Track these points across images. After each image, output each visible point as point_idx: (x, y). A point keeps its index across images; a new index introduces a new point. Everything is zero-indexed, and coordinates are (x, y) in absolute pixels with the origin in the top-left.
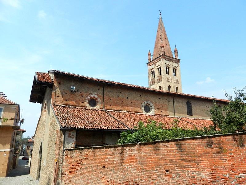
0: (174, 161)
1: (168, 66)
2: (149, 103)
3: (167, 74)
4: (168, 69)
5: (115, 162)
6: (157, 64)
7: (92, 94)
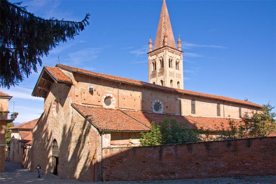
0: (203, 157)
2: (158, 101)
3: (170, 67)
4: (170, 61)
5: (154, 159)
6: (160, 55)
7: (107, 93)
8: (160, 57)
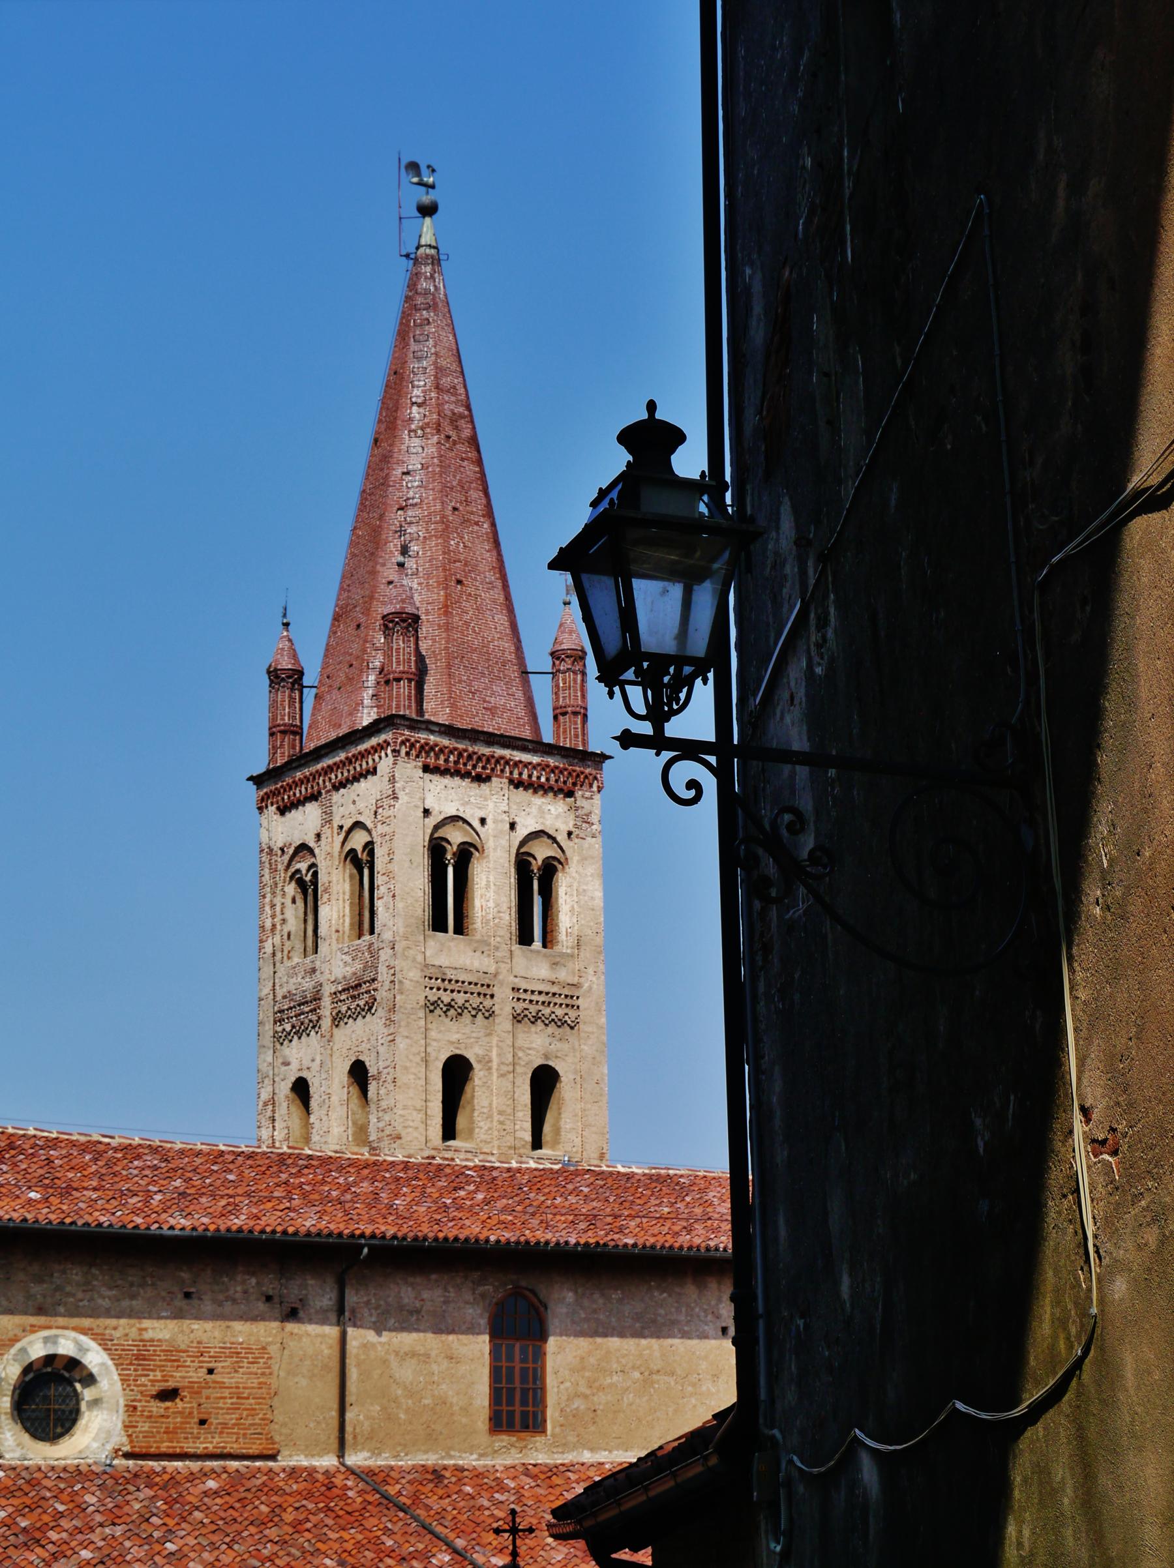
1: (456, 836)
3: (438, 924)
8: (347, 824)
